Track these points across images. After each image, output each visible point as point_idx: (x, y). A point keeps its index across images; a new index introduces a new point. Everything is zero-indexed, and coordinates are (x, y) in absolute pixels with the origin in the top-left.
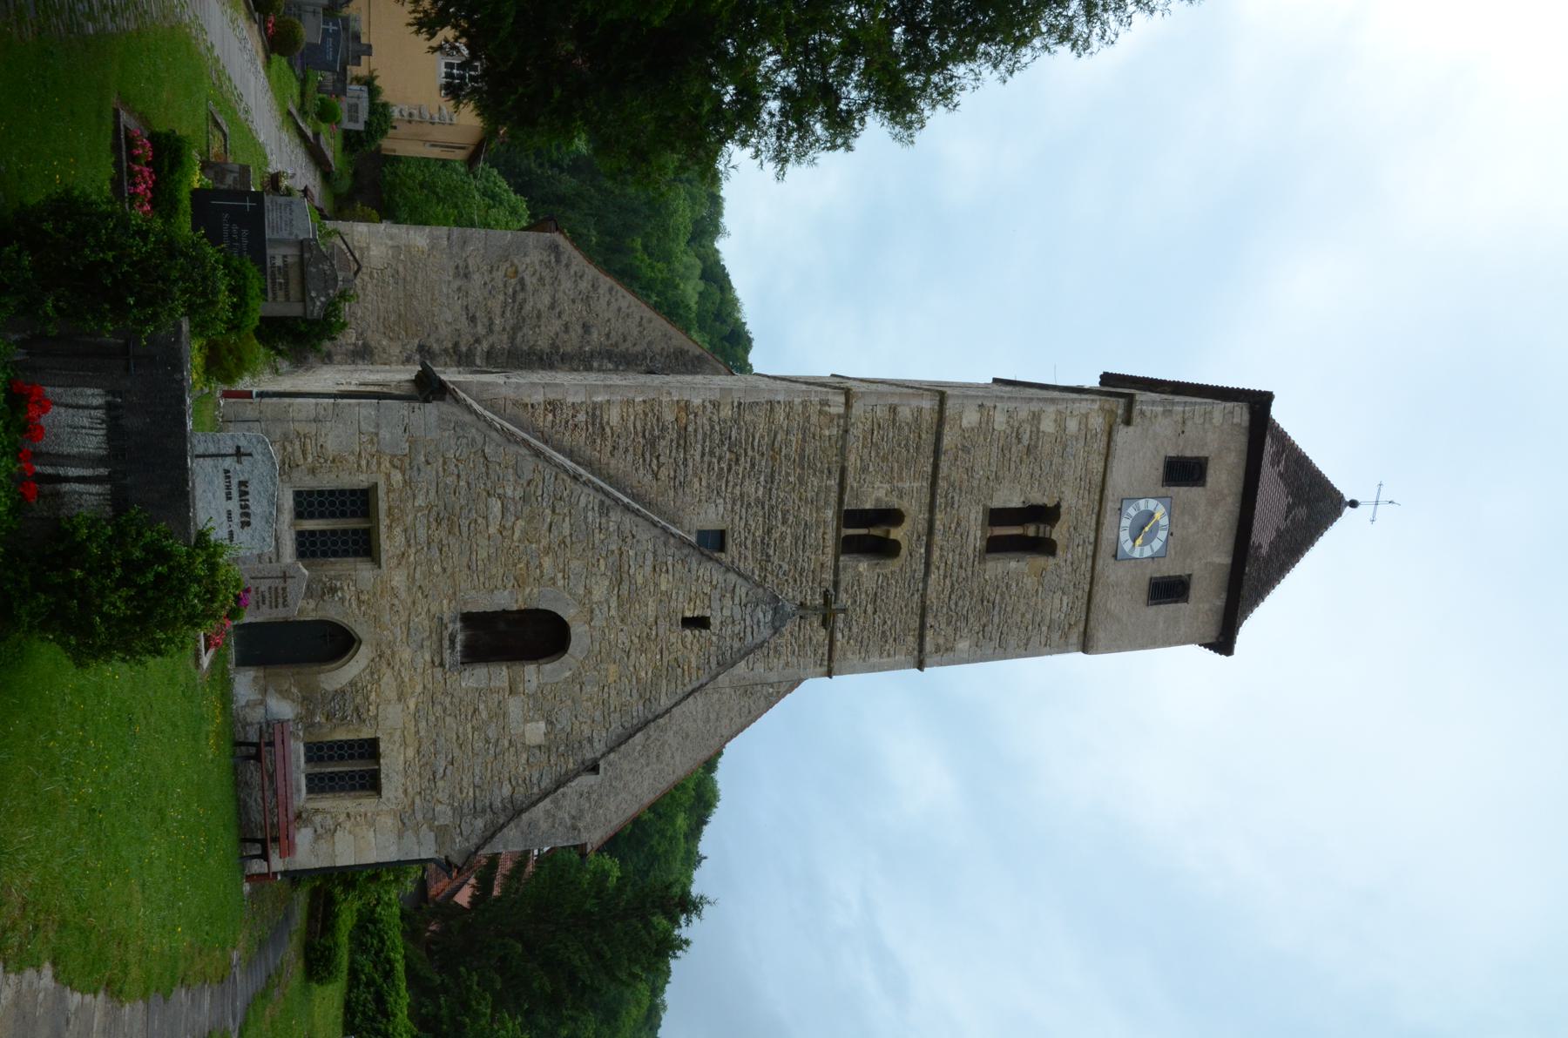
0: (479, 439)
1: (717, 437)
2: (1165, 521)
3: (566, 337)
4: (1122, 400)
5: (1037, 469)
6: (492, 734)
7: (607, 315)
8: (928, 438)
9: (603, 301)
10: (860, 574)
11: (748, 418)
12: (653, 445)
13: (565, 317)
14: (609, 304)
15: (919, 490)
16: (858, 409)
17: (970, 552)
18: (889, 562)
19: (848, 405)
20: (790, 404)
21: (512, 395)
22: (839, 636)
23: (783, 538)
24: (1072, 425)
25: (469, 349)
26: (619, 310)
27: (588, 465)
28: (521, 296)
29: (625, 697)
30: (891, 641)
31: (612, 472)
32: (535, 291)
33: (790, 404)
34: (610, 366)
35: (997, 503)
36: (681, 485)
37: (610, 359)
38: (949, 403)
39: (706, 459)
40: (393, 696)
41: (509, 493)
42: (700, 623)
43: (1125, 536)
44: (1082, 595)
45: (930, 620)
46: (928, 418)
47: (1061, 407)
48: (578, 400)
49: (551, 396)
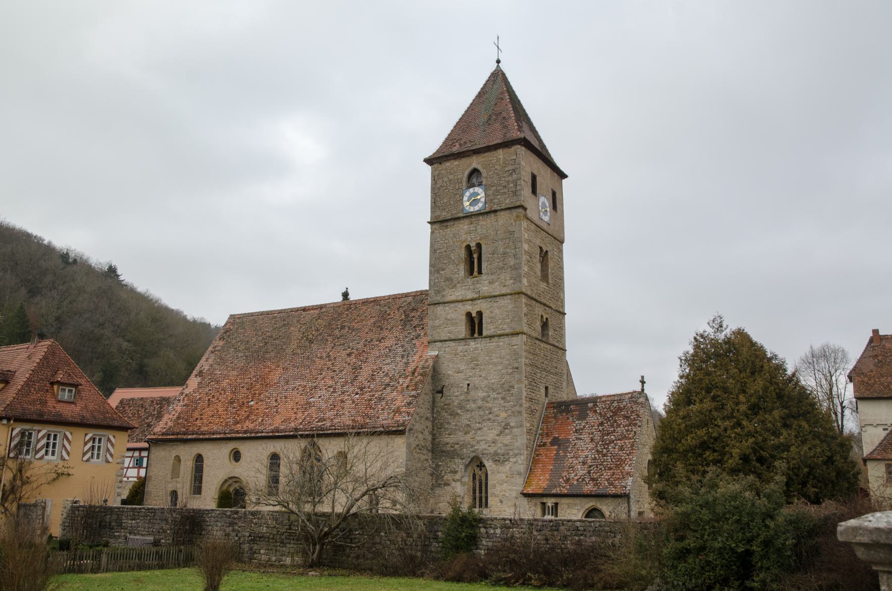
24: (526, 236)
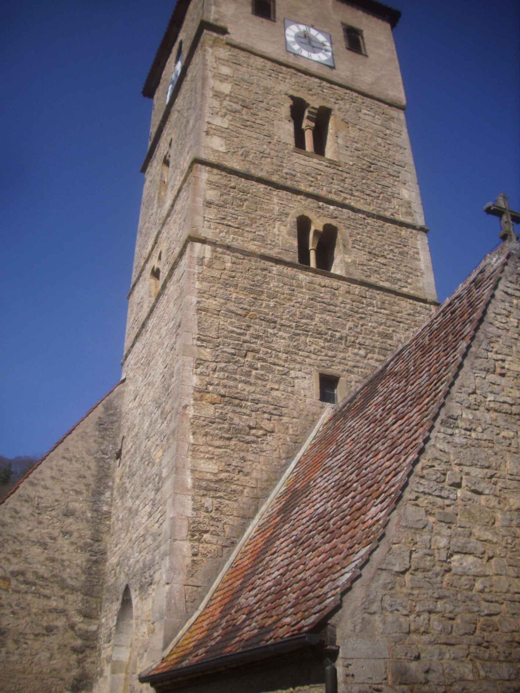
0: (384, 577)
1: (231, 367)
2: (303, 28)
3: (76, 534)
4: (205, 31)
5: (261, 105)
7: (58, 491)
8: (234, 181)
9: (43, 493)
10: (354, 262)
11: (213, 334)
12: (238, 431)
13: (56, 533)
14: (46, 488)
15: (281, 199)
16: (206, 232)
17: (332, 171)
18: (339, 236)
19: (204, 241)
20: (201, 293)
21: (181, 578)
22: (405, 290)
23: (325, 322)
25: (80, 636)
26: (53, 478)
27: (257, 500)
28: (30, 577)
30: (406, 249)
31: (265, 476)
32: (26, 560)
33: (201, 293)
34: (108, 494)
35: (291, 140)
36: (277, 410)
37: (101, 494)
38: (203, 156)
39: (252, 380)
41: (443, 542)
43: (315, 57)
44: (360, 99)
45: (388, 214)
46: (216, 176)
47: (210, 74)
48: (189, 504)
49: (184, 532)
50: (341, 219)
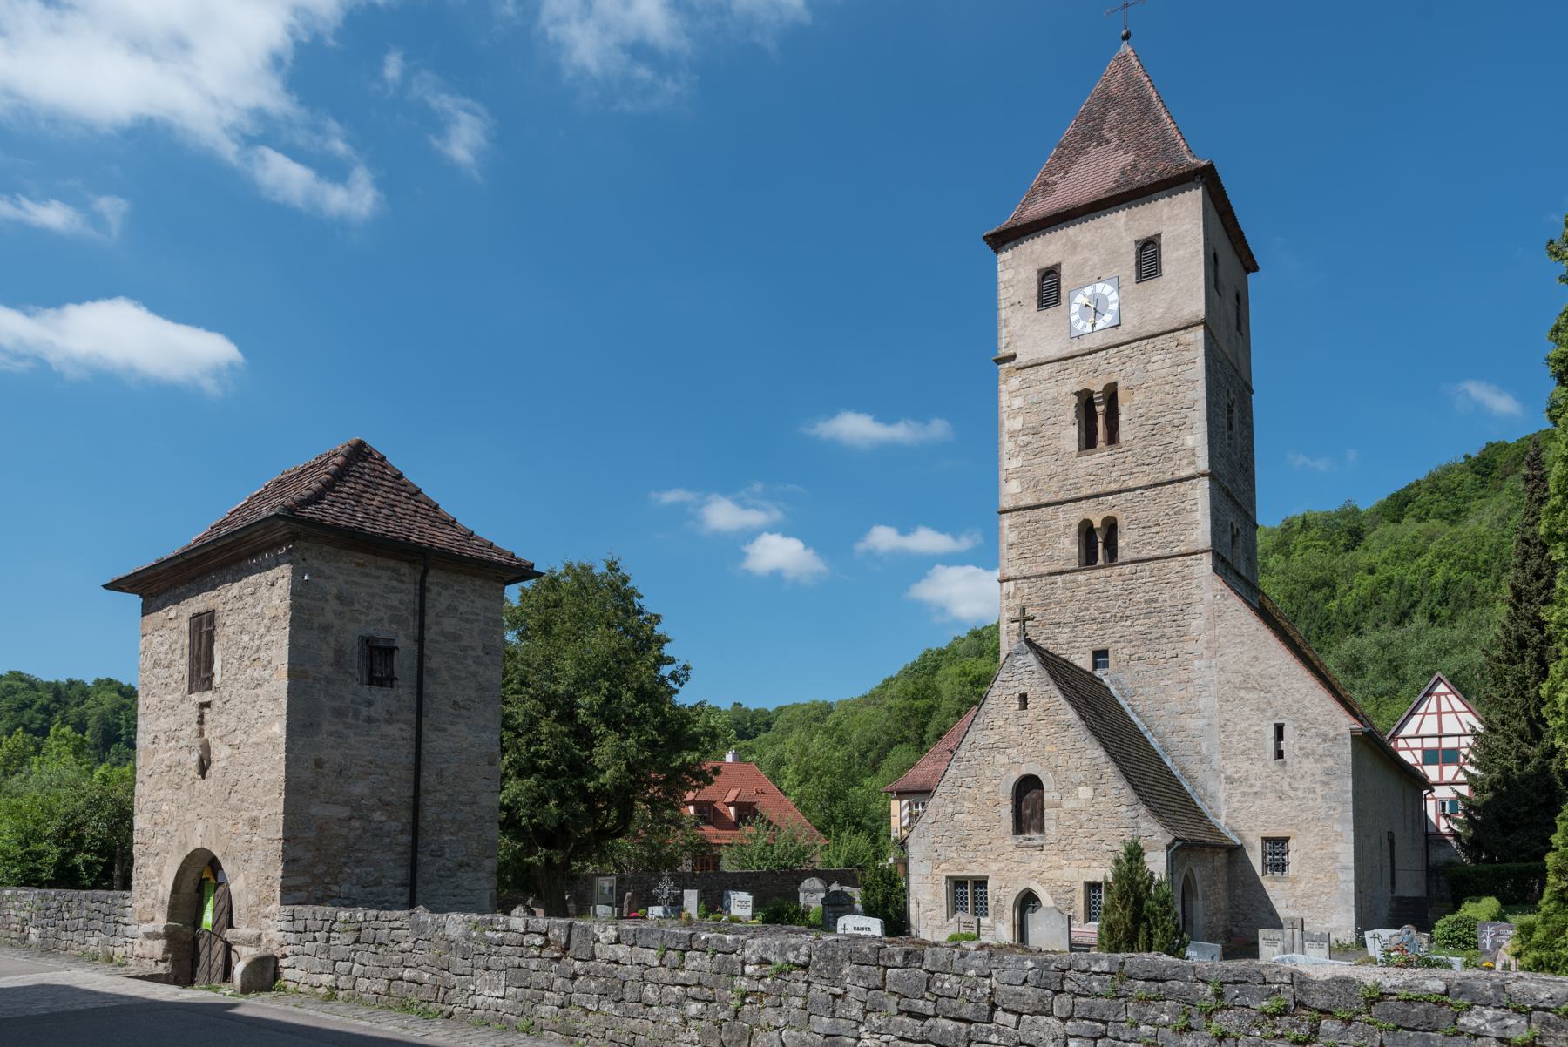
6: (1084, 817)
22: (1176, 550)
29: (1066, 740)
40: (1059, 872)
42: (1024, 698)
50: (1116, 507)
